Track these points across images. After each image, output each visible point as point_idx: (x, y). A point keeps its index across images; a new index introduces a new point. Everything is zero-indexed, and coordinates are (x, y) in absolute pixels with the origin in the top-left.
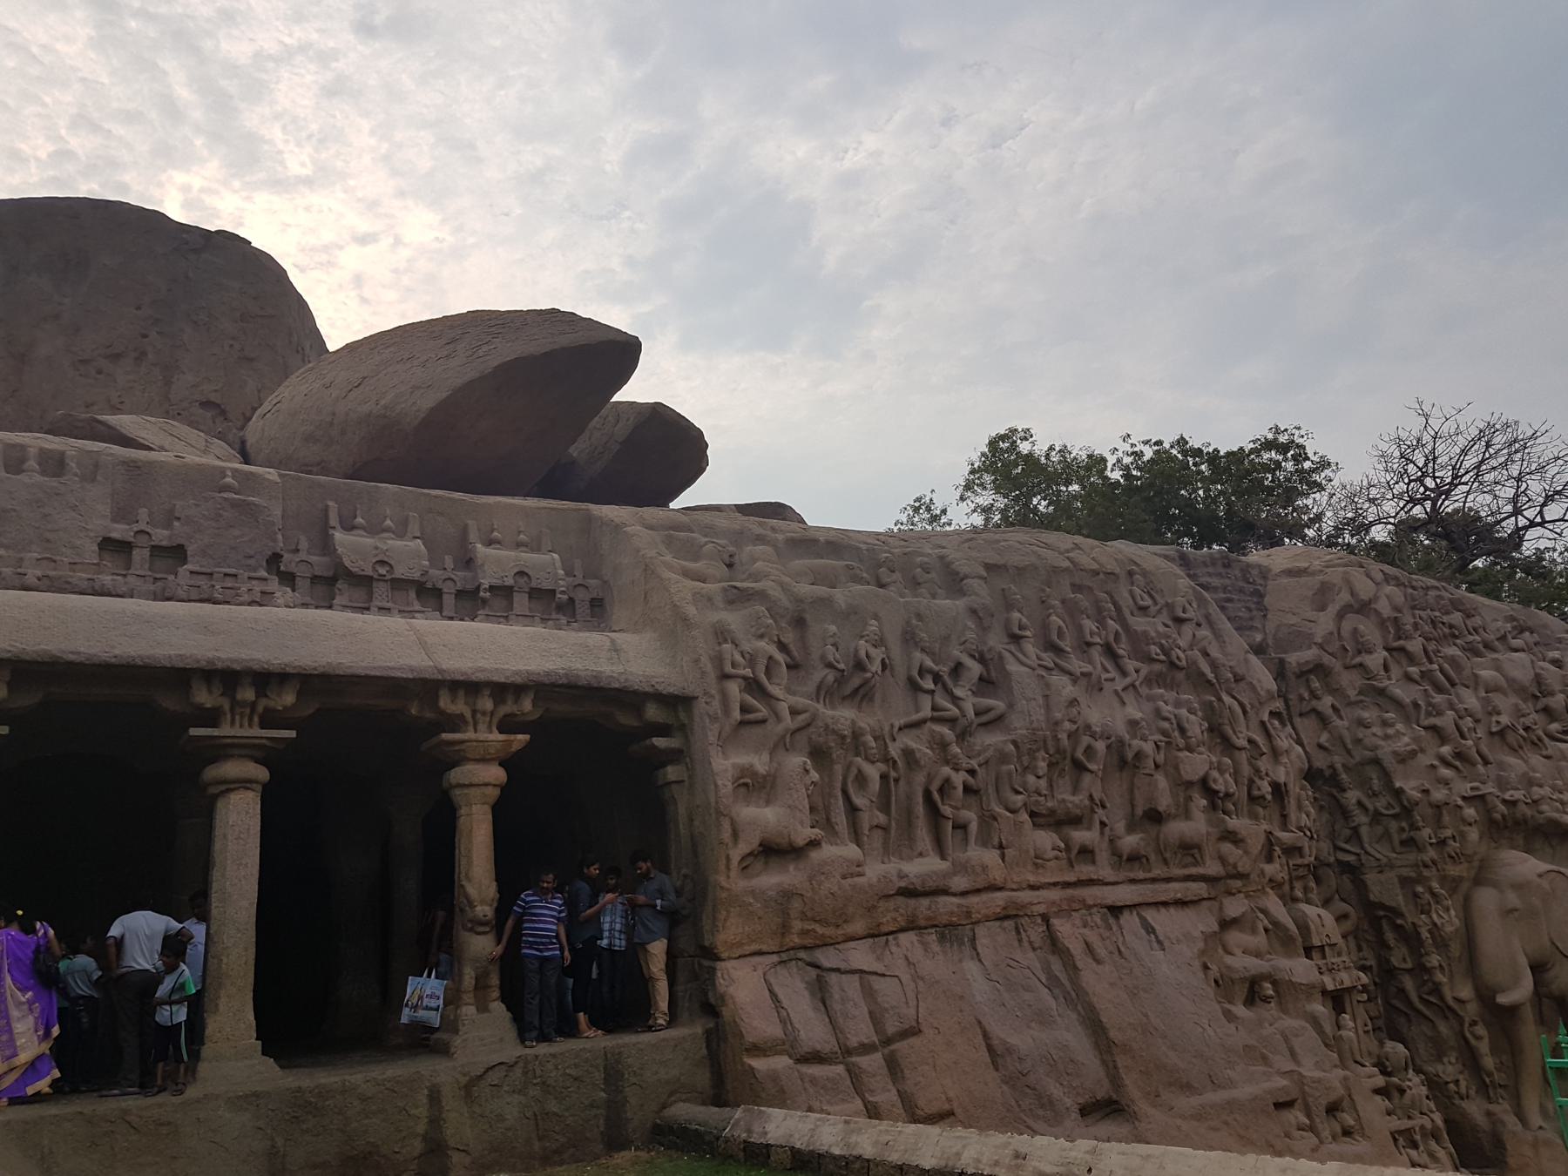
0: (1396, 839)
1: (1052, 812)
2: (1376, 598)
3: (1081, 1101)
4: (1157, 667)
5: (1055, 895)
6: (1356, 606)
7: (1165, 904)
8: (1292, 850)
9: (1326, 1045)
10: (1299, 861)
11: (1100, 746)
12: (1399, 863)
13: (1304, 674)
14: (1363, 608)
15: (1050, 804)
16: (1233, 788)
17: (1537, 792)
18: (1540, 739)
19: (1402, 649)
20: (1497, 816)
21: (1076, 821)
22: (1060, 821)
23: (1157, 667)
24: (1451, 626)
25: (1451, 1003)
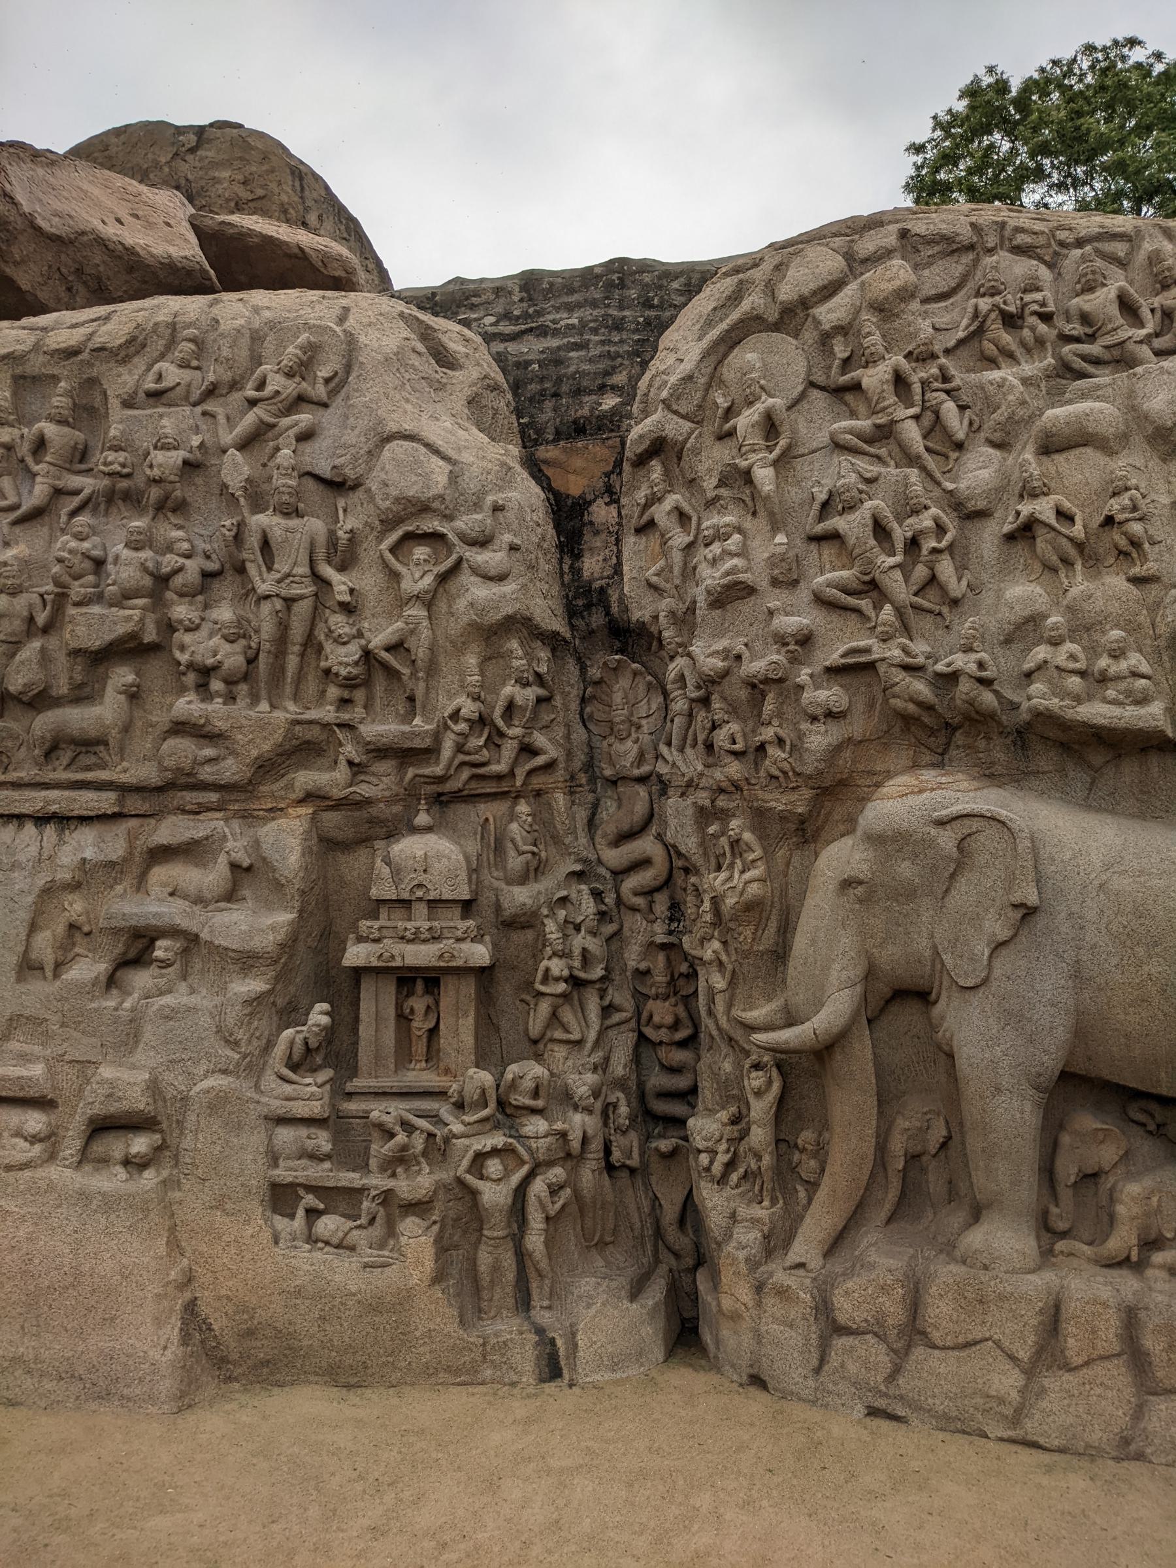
0: (701, 738)
2: (830, 289)
4: (106, 482)
6: (773, 315)
7: (41, 820)
8: (404, 755)
9: (227, 1041)
10: (426, 771)
12: (704, 782)
13: (642, 461)
14: (790, 317)
16: (231, 657)
17: (1041, 652)
18: (1135, 543)
19: (856, 387)
20: (897, 703)
23: (106, 482)
24: (1085, 319)
25: (723, 1021)
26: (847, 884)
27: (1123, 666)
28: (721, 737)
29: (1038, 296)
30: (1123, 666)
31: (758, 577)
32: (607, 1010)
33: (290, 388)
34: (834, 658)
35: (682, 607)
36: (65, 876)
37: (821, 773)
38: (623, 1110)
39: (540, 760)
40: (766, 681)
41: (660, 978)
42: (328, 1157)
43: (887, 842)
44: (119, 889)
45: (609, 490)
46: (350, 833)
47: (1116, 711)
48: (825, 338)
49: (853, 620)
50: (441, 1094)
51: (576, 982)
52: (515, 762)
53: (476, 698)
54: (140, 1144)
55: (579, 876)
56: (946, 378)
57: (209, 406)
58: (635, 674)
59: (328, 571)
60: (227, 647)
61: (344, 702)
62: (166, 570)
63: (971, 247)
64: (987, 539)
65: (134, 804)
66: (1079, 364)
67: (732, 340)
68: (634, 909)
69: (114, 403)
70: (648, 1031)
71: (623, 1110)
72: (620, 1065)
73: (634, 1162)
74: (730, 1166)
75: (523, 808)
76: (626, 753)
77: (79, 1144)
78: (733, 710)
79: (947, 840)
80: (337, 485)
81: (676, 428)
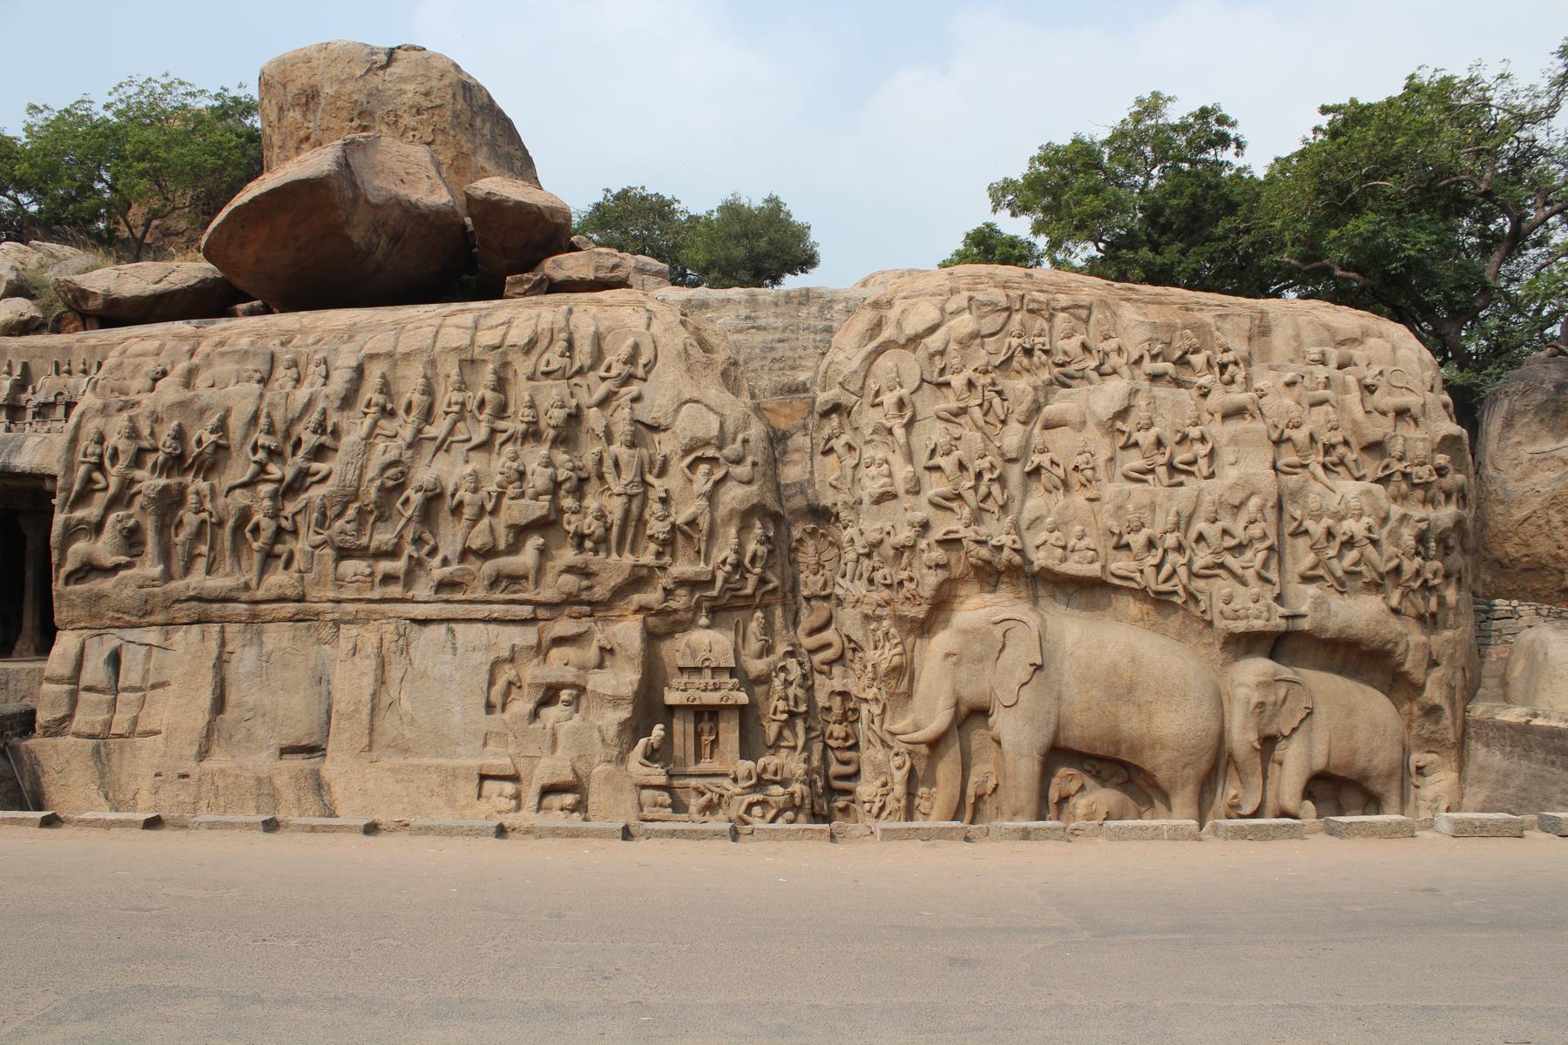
0: (866, 575)
1: (367, 548)
2: (932, 330)
3: (285, 743)
5: (351, 607)
6: (902, 341)
7: (487, 621)
8: (692, 584)
11: (416, 498)
13: (825, 415)
15: (364, 541)
17: (1044, 536)
19: (948, 384)
20: (973, 560)
21: (393, 554)
22: (381, 555)
24: (1065, 353)
26: (948, 655)
27: (1083, 544)
28: (878, 576)
29: (1041, 340)
30: (1083, 544)
31: (900, 488)
32: (808, 730)
33: (627, 369)
34: (937, 533)
35: (851, 501)
36: (506, 654)
37: (934, 597)
38: (819, 784)
39: (771, 586)
40: (904, 547)
41: (837, 710)
42: (670, 806)
43: (970, 633)
44: (535, 661)
45: (805, 427)
46: (663, 629)
47: (1079, 567)
48: (932, 356)
49: (948, 513)
50: (725, 775)
51: (792, 715)
52: (755, 590)
53: (736, 552)
54: (569, 799)
55: (791, 654)
56: (994, 384)
57: (576, 380)
58: (823, 535)
59: (650, 478)
60: (596, 524)
61: (659, 555)
62: (560, 479)
63: (1008, 309)
64: (1015, 473)
65: (542, 613)
66: (1063, 379)
67: (879, 352)
68: (821, 672)
69: (522, 378)
70: (831, 742)
71: (819, 784)
72: (816, 763)
73: (826, 811)
74: (882, 808)
75: (759, 614)
76: (815, 583)
77: (536, 800)
78: (884, 561)
79: (998, 631)
80: (655, 429)
81: (847, 399)
